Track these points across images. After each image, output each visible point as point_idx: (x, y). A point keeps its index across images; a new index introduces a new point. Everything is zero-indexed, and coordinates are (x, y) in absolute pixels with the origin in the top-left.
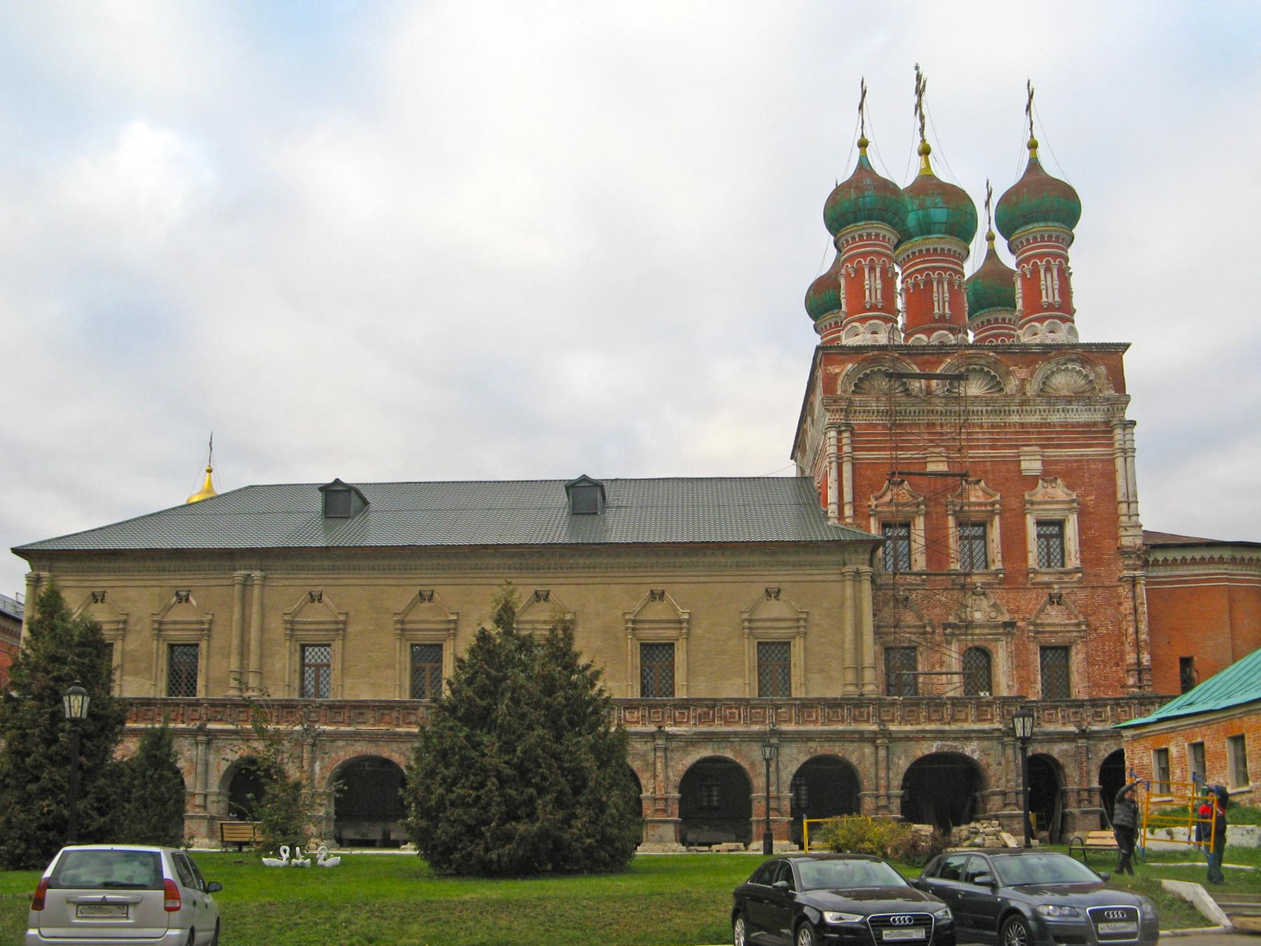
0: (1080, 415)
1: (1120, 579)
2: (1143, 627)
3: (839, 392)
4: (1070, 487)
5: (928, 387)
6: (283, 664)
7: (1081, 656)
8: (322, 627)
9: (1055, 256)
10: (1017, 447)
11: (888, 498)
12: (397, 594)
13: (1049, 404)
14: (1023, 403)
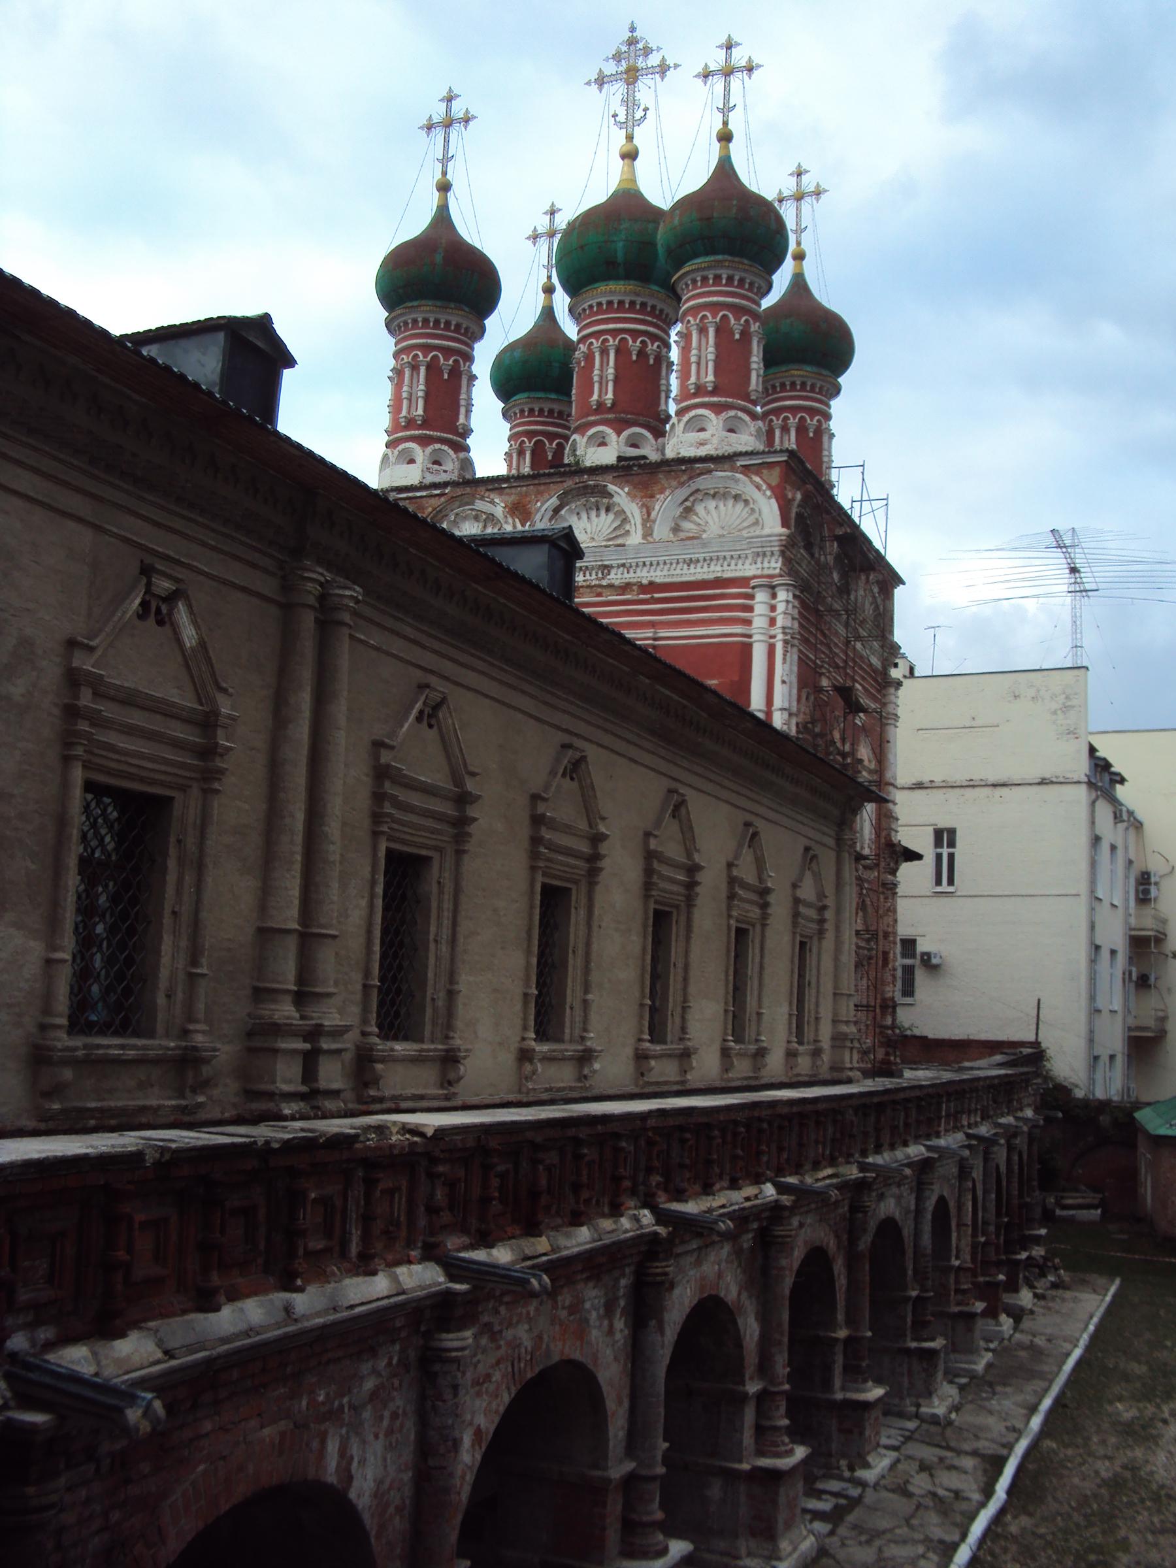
9: (812, 412)
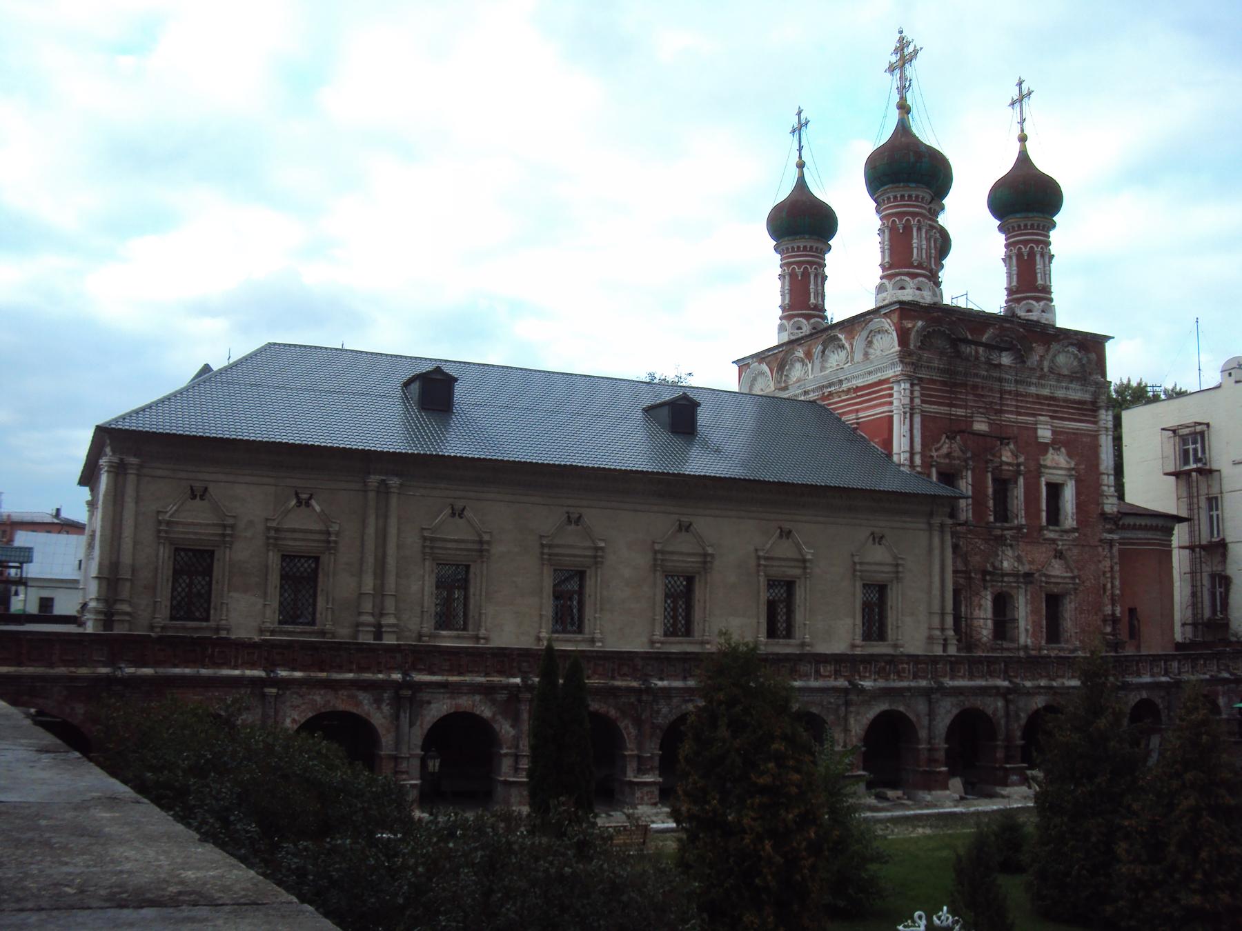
0: (1076, 393)
1: (1101, 540)
2: (1117, 583)
3: (912, 347)
4: (1070, 455)
5: (977, 352)
6: (420, 587)
7: (1073, 605)
8: (463, 546)
9: (1037, 242)
10: (1034, 415)
11: (945, 450)
12: (544, 517)
13: (1058, 381)
14: (1042, 377)
